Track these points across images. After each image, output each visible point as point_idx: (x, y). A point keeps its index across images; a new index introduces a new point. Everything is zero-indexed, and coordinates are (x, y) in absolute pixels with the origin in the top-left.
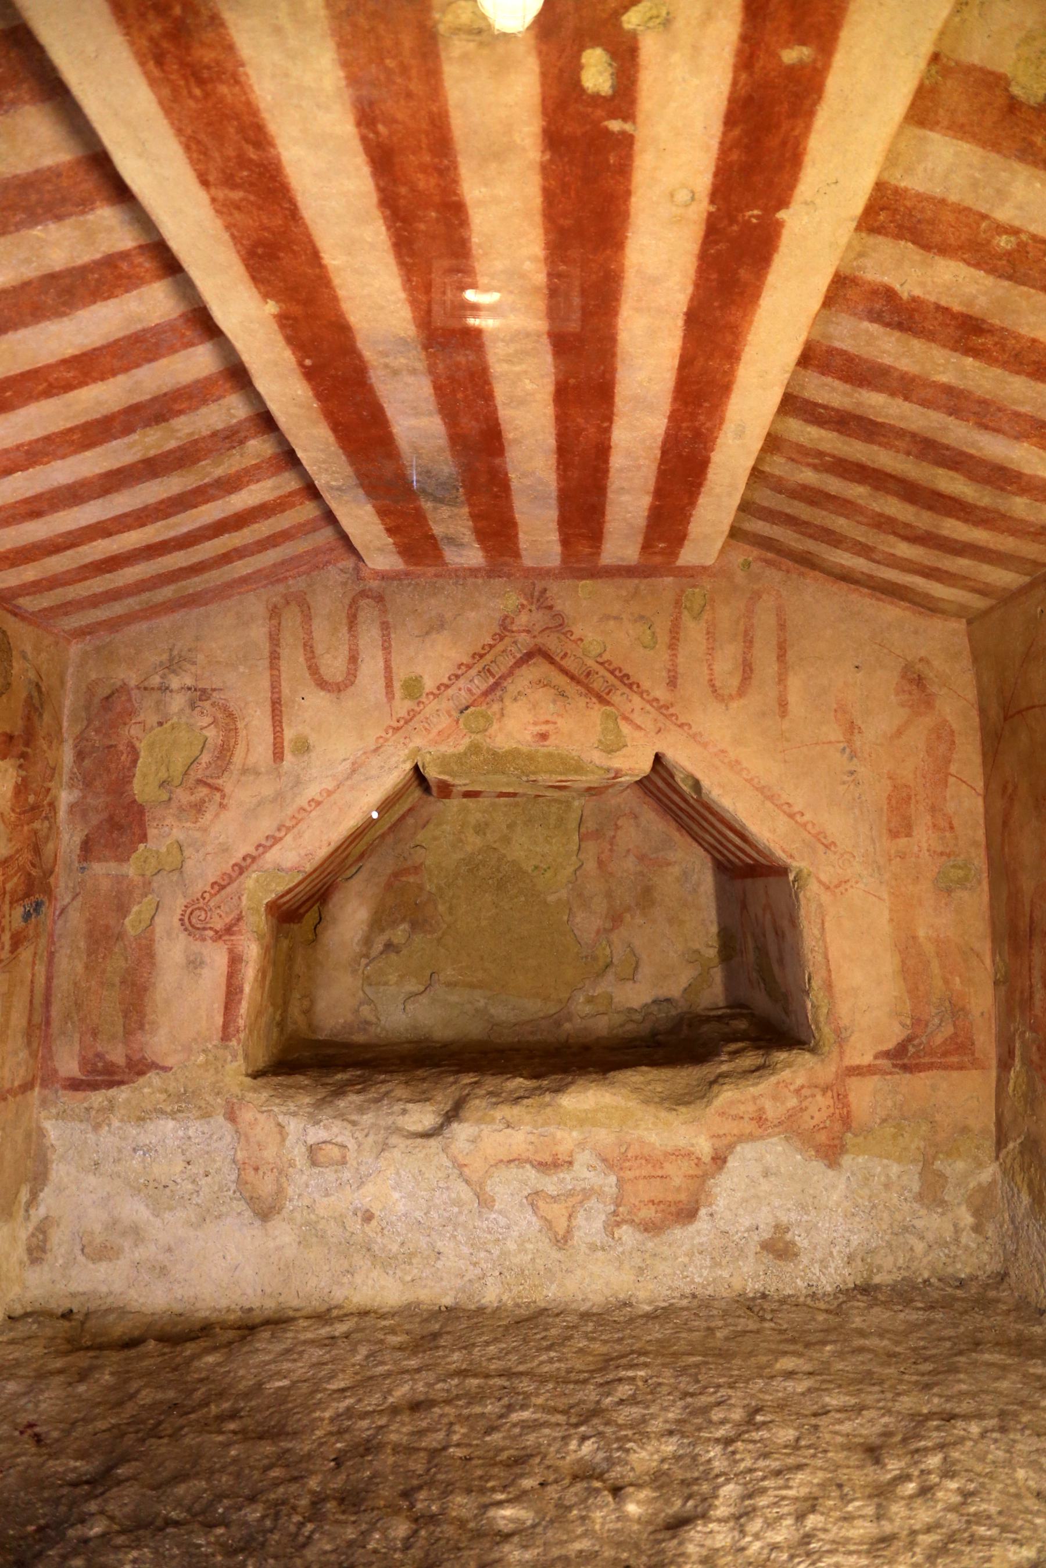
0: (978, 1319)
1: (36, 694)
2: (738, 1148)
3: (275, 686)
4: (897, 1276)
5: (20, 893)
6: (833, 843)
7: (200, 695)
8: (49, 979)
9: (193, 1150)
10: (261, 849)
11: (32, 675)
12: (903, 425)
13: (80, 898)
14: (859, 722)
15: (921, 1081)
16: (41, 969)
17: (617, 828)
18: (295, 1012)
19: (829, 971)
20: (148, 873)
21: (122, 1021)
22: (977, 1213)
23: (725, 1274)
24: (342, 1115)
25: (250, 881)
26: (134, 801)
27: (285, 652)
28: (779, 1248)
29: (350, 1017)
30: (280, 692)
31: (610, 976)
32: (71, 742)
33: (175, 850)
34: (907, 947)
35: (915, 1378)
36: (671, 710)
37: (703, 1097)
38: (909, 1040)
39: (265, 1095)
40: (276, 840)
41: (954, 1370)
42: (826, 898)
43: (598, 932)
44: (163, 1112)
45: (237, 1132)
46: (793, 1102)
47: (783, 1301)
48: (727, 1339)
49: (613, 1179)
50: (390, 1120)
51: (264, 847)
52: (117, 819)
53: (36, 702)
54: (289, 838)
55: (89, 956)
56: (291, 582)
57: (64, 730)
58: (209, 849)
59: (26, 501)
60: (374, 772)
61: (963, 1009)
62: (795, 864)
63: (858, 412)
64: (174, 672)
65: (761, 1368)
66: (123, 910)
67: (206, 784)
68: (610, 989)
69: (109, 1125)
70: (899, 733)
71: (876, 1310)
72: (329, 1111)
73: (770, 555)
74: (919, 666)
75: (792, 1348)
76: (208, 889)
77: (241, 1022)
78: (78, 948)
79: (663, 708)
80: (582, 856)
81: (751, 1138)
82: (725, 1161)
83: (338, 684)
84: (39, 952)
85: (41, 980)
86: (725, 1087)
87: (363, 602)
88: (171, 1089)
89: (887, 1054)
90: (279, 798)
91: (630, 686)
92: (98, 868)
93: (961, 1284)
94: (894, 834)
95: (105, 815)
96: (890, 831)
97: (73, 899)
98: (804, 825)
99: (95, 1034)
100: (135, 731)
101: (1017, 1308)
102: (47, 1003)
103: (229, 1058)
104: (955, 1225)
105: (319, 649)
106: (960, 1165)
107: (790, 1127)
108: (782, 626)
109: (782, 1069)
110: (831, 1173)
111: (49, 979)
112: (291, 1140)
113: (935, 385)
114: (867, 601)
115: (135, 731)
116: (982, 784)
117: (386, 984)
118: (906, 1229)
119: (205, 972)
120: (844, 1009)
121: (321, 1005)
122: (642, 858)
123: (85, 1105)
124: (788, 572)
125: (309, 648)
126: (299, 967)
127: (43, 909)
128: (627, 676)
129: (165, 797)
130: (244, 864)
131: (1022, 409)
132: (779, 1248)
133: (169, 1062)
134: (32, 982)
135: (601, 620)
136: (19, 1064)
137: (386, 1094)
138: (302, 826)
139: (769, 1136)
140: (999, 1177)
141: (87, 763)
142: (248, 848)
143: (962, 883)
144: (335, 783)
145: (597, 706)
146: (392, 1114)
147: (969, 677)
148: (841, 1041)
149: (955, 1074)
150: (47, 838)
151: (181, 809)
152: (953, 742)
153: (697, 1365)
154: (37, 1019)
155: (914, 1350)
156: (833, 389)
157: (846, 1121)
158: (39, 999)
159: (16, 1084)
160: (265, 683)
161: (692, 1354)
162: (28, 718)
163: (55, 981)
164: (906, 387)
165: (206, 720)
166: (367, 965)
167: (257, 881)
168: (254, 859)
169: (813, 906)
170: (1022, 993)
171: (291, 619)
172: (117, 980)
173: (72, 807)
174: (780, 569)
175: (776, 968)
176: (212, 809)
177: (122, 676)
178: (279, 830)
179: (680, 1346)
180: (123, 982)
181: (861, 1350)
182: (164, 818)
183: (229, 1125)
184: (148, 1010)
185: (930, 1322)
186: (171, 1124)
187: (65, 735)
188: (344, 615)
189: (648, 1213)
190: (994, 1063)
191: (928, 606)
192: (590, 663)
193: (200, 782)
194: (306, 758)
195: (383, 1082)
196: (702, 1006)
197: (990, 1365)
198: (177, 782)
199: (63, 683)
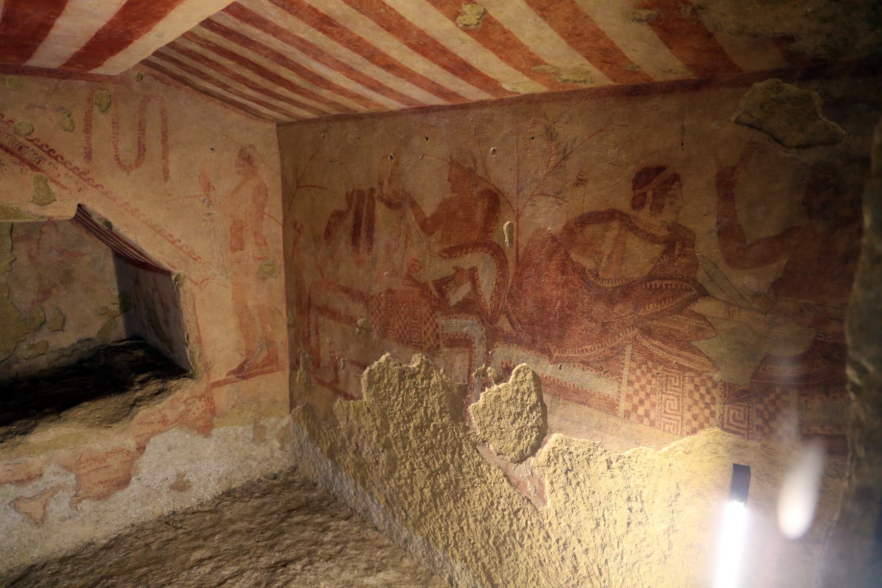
0: (287, 495)
2: (152, 439)
4: (244, 481)
6: (199, 257)
12: (268, 45)
14: (214, 184)
15: (252, 383)
17: (41, 233)
19: (199, 332)
22: (282, 441)
23: (150, 508)
28: (181, 486)
31: (45, 330)
34: (242, 312)
35: (264, 543)
36: (89, 176)
37: (127, 415)
38: (245, 362)
41: (282, 533)
42: (196, 290)
43: (33, 303)
46: (182, 408)
47: (185, 513)
48: (159, 549)
49: (73, 476)
61: (272, 342)
62: (176, 272)
63: (241, 33)
65: (183, 563)
68: (46, 339)
70: (237, 190)
71: (237, 504)
73: (156, 72)
74: (249, 150)
75: (196, 544)
79: (82, 174)
80: (15, 253)
81: (160, 432)
82: (144, 448)
86: (141, 408)
89: (233, 372)
91: (56, 158)
93: (275, 477)
94: (234, 249)
96: (232, 248)
98: (181, 248)
101: (303, 485)
104: (271, 449)
106: (273, 420)
107: (182, 421)
108: (164, 121)
109: (175, 391)
110: (206, 440)
113: (295, 36)
114: (219, 108)
116: (281, 218)
118: (247, 458)
120: (209, 351)
122: (62, 252)
124: (169, 84)
128: (53, 151)
131: (342, 60)
132: (181, 486)
135: (27, 108)
139: (170, 429)
140: (291, 421)
143: (271, 274)
145: (30, 172)
147: (276, 157)
148: (208, 369)
149: (269, 376)
152: (267, 195)
153: (145, 575)
155: (260, 524)
156: (227, 18)
157: (213, 412)
161: (141, 567)
164: (276, 31)
169: (188, 295)
170: (304, 334)
174: (163, 83)
175: (162, 324)
179: (132, 563)
181: (234, 533)
185: (264, 504)
189: (97, 490)
190: (288, 366)
191: (258, 116)
192: (21, 139)
196: (111, 340)
197: (298, 523)
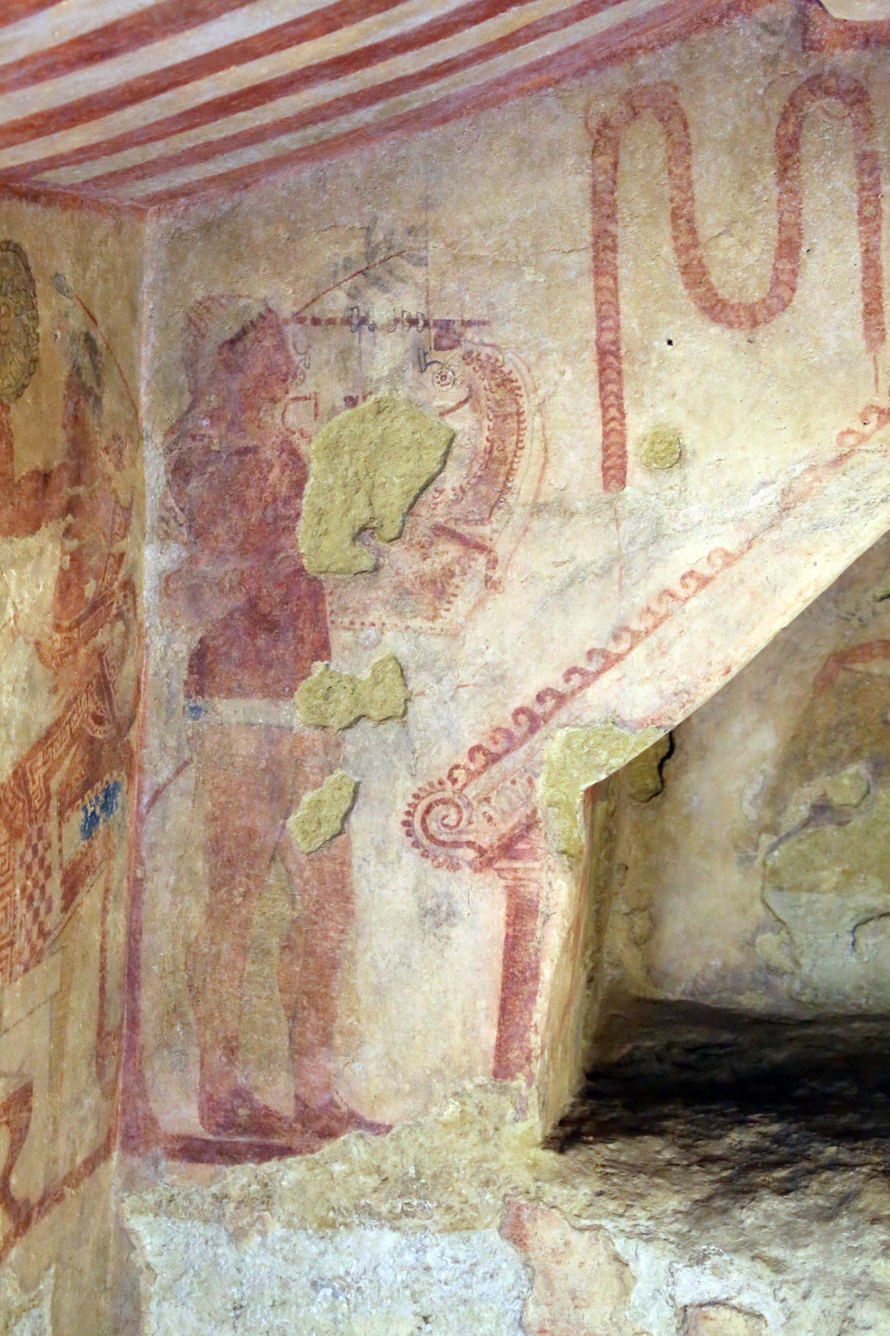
1: (85, 361)
3: (607, 311)
5: (76, 784)
7: (438, 337)
8: (134, 934)
9: (436, 1293)
10: (576, 680)
11: (77, 322)
13: (191, 772)
16: (118, 918)
18: (618, 939)
20: (334, 723)
21: (285, 1027)
24: (751, 1245)
25: (552, 744)
26: (301, 571)
27: (627, 233)
29: (735, 956)
30: (617, 328)
32: (158, 439)
33: (391, 678)
39: (585, 1191)
40: (610, 660)
44: (372, 1213)
45: (526, 1265)
50: (857, 1265)
51: (583, 673)
52: (264, 608)
53: (88, 377)
54: (639, 652)
55: (214, 889)
56: (642, 61)
57: (142, 413)
58: (464, 675)
59: (82, 40)
60: (831, 512)
64: (377, 282)
66: (282, 799)
67: (450, 536)
69: (263, 1234)
72: (722, 1234)
76: (463, 759)
77: (535, 1041)
78: (191, 871)
83: (751, 309)
84: (114, 885)
85: (119, 938)
87: (814, 107)
88: (387, 1167)
90: (615, 566)
92: (228, 710)
95: (239, 600)
97: (178, 772)
99: (231, 1050)
100: (295, 416)
102: (132, 978)
103: (510, 1113)
105: (709, 223)
111: (134, 934)
112: (640, 1291)
115: (295, 416)
117: (813, 888)
119: (459, 933)
121: (673, 928)
123: (214, 1189)
125: (683, 220)
126: (627, 849)
127: (119, 798)
129: (366, 562)
130: (539, 710)
133: (385, 1114)
134: (103, 950)
136: (83, 1121)
137: (846, 1200)
138: (668, 630)
141: (195, 486)
142: (548, 676)
144: (743, 536)
146: (860, 1251)
150: (122, 656)
151: (402, 591)
154: (112, 1021)
158: (115, 976)
159: (79, 1160)
160: (586, 309)
162: (76, 420)
163: (146, 938)
165: (452, 395)
166: (773, 848)
167: (568, 744)
168: (561, 699)
171: (644, 152)
172: (274, 943)
173: (167, 580)
176: (468, 590)
177: (262, 292)
178: (616, 638)
180: (287, 947)
182: (366, 609)
183: (510, 1250)
184: (341, 1006)
186: (390, 1238)
187: (146, 425)
188: (769, 139)
193: (440, 531)
194: (675, 479)
195: (834, 1165)
198: (390, 531)
199: (134, 310)
